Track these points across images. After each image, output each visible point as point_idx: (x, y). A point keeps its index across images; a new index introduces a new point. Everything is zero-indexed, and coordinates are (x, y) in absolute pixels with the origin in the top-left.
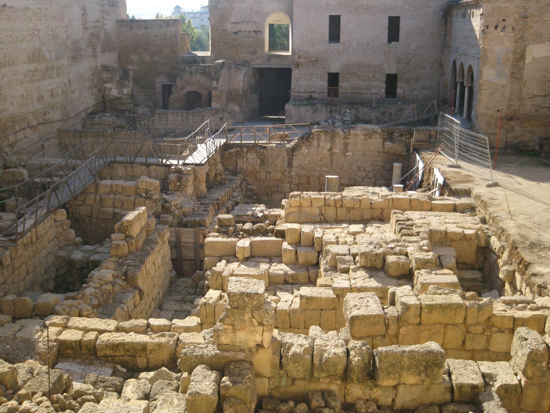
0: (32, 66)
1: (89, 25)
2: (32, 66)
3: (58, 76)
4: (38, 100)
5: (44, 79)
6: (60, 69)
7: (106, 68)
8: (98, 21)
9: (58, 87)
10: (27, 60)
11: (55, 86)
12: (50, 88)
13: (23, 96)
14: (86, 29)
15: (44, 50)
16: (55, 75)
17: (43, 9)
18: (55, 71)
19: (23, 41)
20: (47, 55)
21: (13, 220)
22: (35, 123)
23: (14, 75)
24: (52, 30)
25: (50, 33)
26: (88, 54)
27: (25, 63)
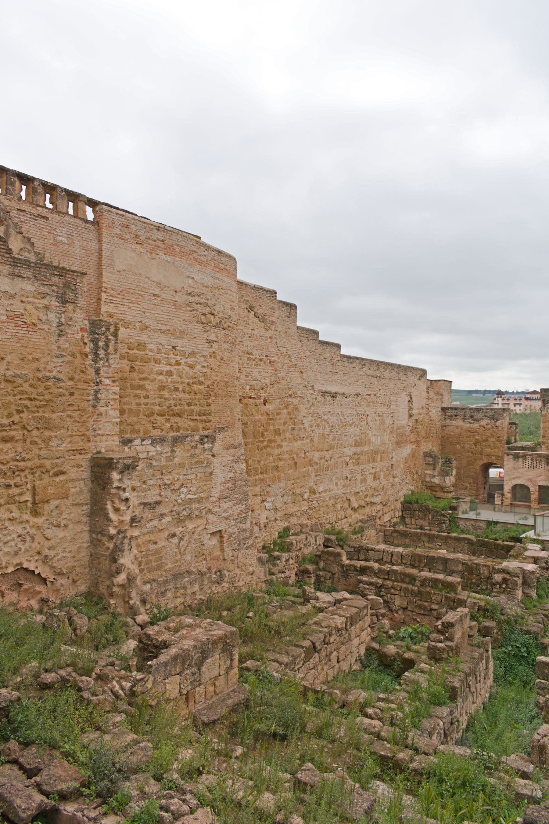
0: (359, 450)
1: (414, 412)
2: (359, 450)
3: (381, 460)
4: (361, 482)
5: (369, 462)
6: (384, 453)
7: (427, 455)
8: (423, 408)
9: (380, 471)
10: (354, 443)
11: (378, 470)
12: (373, 471)
13: (347, 477)
14: (411, 416)
15: (370, 435)
16: (379, 459)
17: (372, 395)
18: (379, 456)
19: (351, 425)
20: (373, 439)
21: (329, 602)
22: (356, 505)
23: (341, 457)
24: (379, 416)
25: (377, 418)
26: (412, 440)
27: (352, 446)
